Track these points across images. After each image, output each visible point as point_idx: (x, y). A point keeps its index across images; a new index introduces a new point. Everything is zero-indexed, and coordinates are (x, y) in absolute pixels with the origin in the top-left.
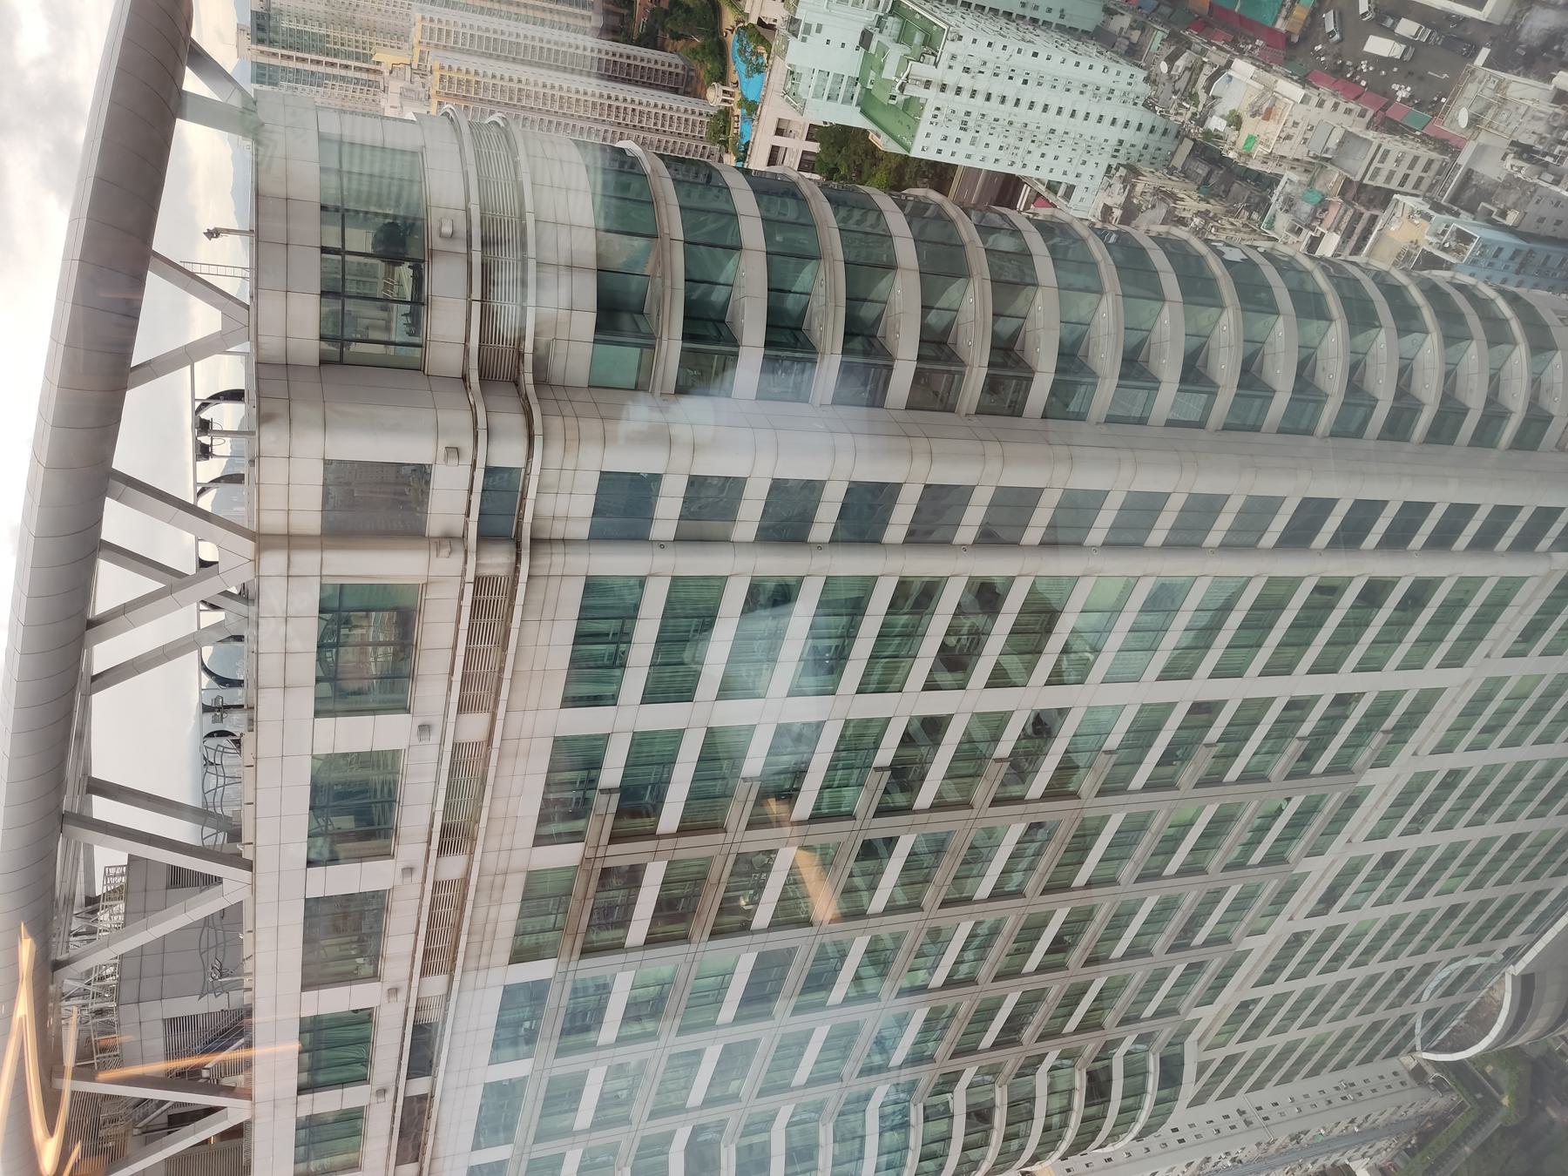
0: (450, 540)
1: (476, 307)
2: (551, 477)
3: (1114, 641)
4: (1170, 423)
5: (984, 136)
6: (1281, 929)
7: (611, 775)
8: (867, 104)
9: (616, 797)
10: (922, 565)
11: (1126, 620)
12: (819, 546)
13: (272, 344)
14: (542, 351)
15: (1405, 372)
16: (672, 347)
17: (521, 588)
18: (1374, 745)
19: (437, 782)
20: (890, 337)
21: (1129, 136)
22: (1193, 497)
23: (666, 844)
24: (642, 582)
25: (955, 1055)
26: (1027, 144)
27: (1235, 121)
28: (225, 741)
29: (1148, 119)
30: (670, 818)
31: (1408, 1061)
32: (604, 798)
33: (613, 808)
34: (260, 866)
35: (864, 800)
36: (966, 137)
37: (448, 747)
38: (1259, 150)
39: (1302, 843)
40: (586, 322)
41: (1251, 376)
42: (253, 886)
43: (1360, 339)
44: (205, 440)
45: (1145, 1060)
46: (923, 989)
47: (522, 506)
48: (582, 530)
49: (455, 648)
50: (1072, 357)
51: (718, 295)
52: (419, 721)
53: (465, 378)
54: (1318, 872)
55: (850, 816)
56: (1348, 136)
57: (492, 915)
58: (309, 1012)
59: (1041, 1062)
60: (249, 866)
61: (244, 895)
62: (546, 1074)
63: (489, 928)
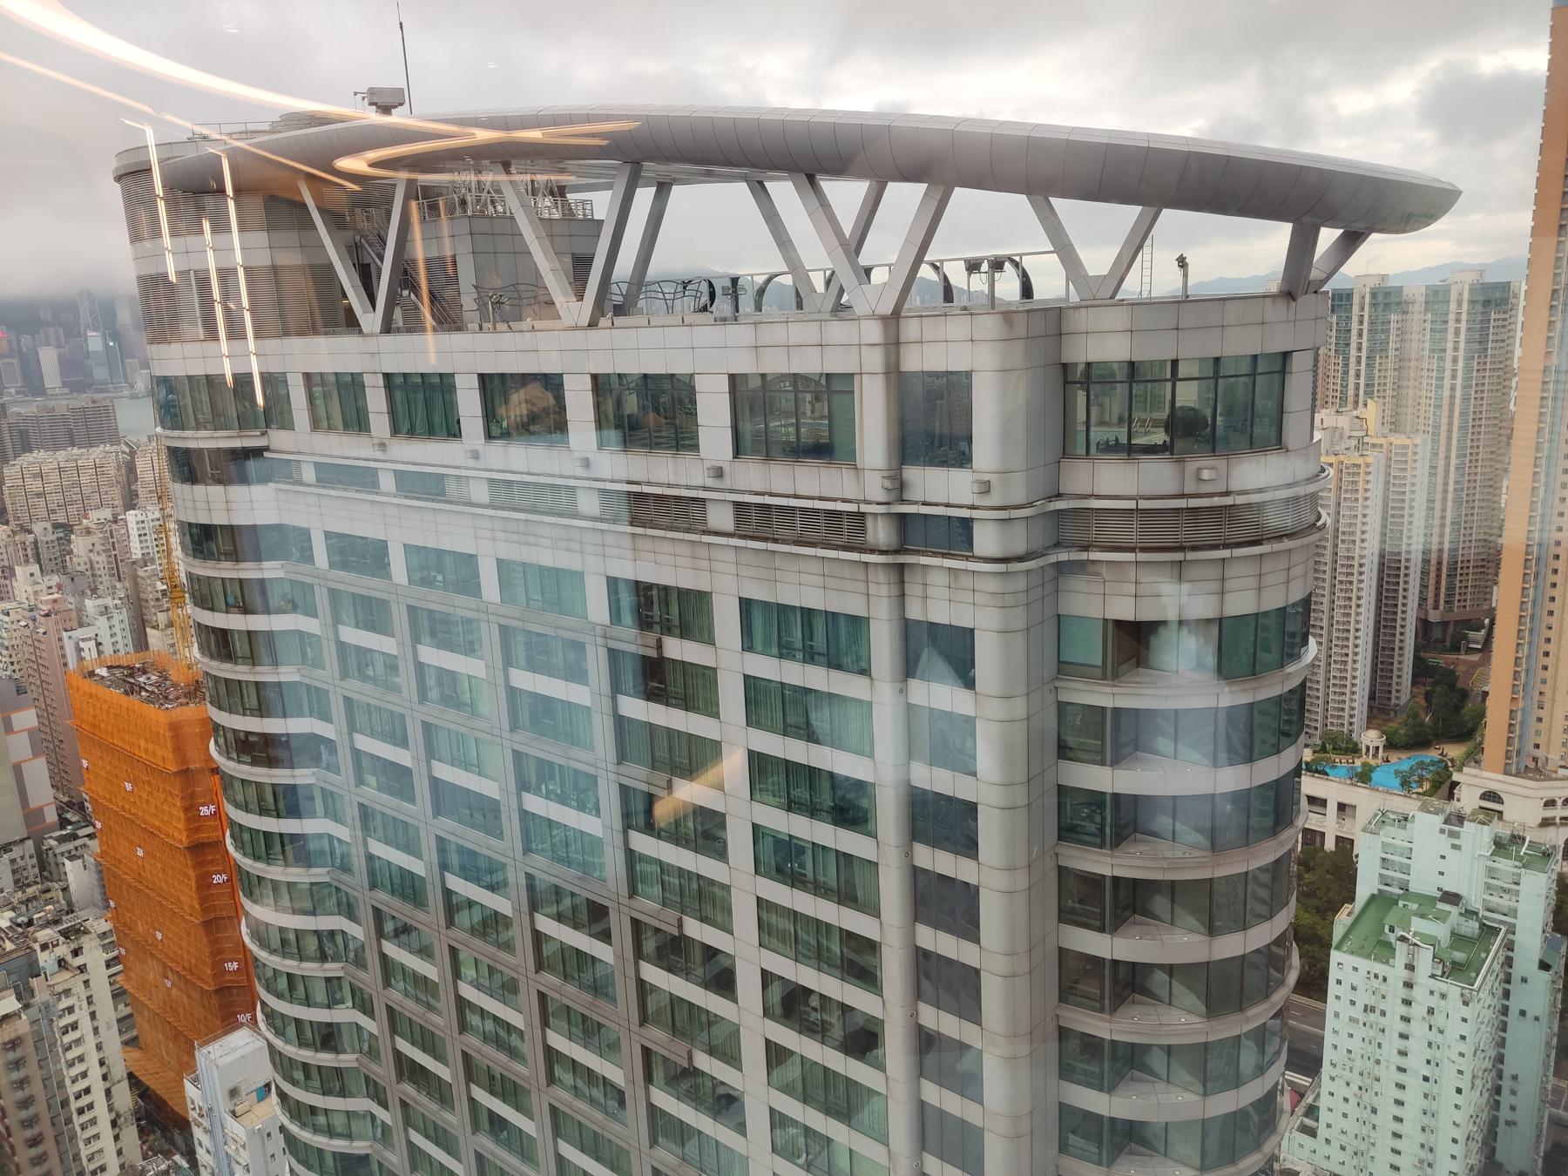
0: (899, 489)
1: (1131, 505)
2: (966, 581)
5: (1360, 1032)
8: (1382, 901)
10: (894, 968)
12: (909, 854)
13: (1081, 320)
14: (1091, 568)
19: (669, 486)
20: (1135, 930)
25: (390, 1010)
28: (705, 299)
32: (653, 642)
34: (592, 333)
35: (648, 907)
36: (1357, 1012)
40: (1124, 610)
42: (576, 328)
44: (985, 267)
46: (457, 975)
47: (935, 554)
48: (914, 612)
49: (796, 497)
51: (1164, 744)
52: (726, 467)
53: (1059, 496)
55: (633, 893)
60: (593, 324)
61: (567, 320)
62: (393, 597)
63: (531, 539)
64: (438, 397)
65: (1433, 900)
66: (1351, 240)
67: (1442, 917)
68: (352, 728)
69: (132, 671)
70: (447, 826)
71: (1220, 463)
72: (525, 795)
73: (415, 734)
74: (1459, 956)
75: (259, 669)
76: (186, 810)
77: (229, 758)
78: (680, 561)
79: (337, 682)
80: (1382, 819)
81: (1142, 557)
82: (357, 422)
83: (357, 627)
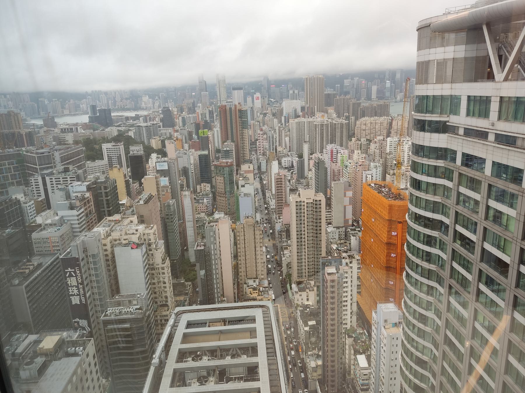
46: (475, 318)
59: (435, 347)
62: (483, 180)
68: (456, 222)
69: (381, 186)
70: (484, 267)
73: (480, 230)
75: (428, 195)
76: (388, 232)
77: (412, 221)
79: (454, 206)
82: (485, 114)
83: (467, 188)
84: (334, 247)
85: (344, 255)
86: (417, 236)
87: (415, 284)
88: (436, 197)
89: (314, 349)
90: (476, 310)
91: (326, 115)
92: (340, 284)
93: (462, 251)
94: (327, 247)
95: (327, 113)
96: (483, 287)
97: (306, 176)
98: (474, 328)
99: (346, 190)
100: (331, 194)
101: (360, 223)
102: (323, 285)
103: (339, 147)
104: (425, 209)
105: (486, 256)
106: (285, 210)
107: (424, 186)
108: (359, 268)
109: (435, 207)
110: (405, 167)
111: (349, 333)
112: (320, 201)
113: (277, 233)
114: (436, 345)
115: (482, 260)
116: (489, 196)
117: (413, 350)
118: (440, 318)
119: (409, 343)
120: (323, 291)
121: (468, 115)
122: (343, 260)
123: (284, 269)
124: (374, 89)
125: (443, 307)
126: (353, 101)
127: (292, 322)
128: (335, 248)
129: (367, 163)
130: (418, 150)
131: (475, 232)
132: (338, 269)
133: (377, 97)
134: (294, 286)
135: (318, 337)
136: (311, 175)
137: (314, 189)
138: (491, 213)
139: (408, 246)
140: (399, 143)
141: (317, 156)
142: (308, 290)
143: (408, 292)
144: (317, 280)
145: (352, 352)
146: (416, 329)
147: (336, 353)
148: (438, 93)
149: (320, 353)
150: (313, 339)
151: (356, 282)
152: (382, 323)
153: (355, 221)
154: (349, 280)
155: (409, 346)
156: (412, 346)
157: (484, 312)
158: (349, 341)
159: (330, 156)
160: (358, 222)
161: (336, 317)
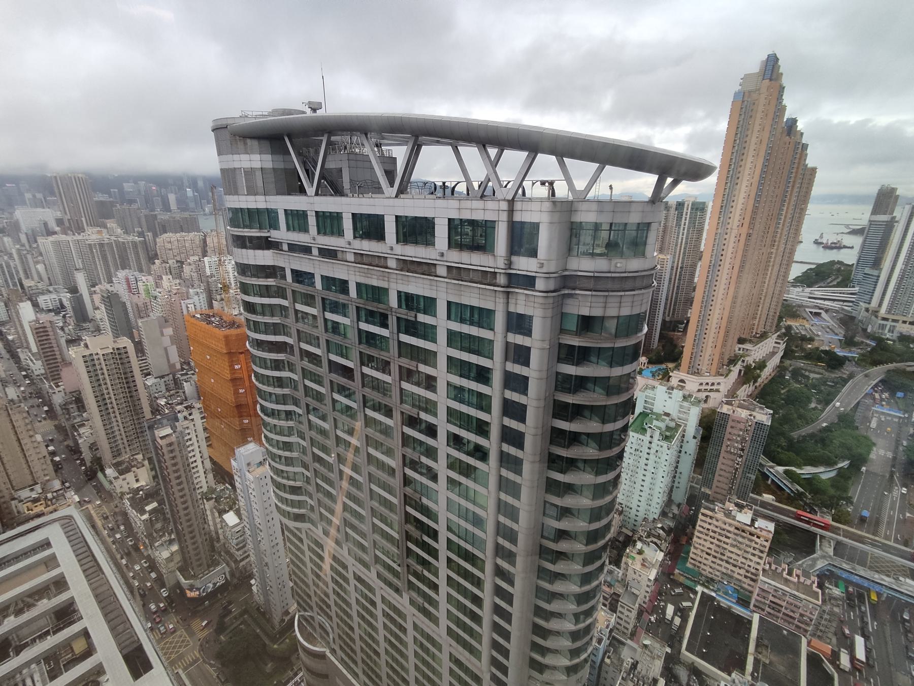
0: (509, 265)
1: (592, 274)
2: (532, 299)
3: (463, 502)
4: (543, 524)
5: (633, 457)
6: (350, 561)
7: (422, 318)
8: (644, 415)
9: (413, 319)
10: (495, 432)
11: (471, 506)
12: (503, 393)
15: (560, 616)
16: (576, 342)
17: (492, 288)
18: (418, 599)
19: (423, 258)
20: (578, 421)
21: (633, 512)
22: (517, 533)
23: (395, 337)
24: (492, 329)
26: (630, 473)
27: (640, 552)
28: (433, 189)
29: (640, 519)
30: (405, 338)
31: (293, 607)
32: (414, 315)
33: (409, 318)
34: (396, 200)
35: (407, 408)
36: (632, 451)
37: (435, 262)
38: (630, 561)
39: (382, 570)
40: (585, 312)
41: (560, 556)
42: (390, 198)
43: (573, 598)
44: (547, 184)
45: (304, 508)
46: (336, 427)
47: (521, 289)
48: (512, 309)
49: (471, 265)
50: (569, 489)
52: (445, 252)
54: (371, 576)
55: (402, 402)
56: (637, 596)
57: (374, 277)
58: (344, 215)
60: (396, 197)
61: (387, 195)
63: (369, 275)
64: (336, 222)
65: (661, 415)
66: (675, 183)
67: (663, 421)
68: (299, 340)
69: (209, 316)
71: (623, 261)
72: (363, 367)
74: (668, 434)
76: (230, 366)
78: (425, 286)
80: (647, 387)
81: (594, 293)
82: (304, 229)
84: (162, 402)
85: (179, 408)
86: (263, 363)
87: (273, 414)
88: (274, 318)
89: (164, 535)
90: (335, 419)
91: (105, 231)
92: (180, 445)
93: (311, 367)
94: (151, 406)
95: (105, 227)
96: (336, 396)
97: (90, 317)
98: (337, 436)
99: (161, 327)
100: (140, 336)
101: (192, 364)
102: (157, 454)
103: (137, 273)
104: (266, 333)
105: (334, 367)
106: (65, 373)
107: (259, 309)
108: (202, 418)
109: (276, 329)
110: (234, 291)
111: (206, 497)
112: (125, 348)
113: (58, 408)
114: (305, 466)
115: (330, 372)
116: (324, 310)
117: (284, 481)
118: (304, 439)
119: (278, 476)
120: (159, 462)
121: (288, 229)
122: (179, 415)
123: (87, 455)
124: (172, 198)
125: (304, 428)
126: (145, 212)
127: (120, 518)
128: (163, 403)
129: (184, 289)
130: (243, 269)
131: (319, 347)
132: (174, 428)
133: (178, 208)
134: (110, 472)
135: (165, 519)
136: (101, 315)
137: (111, 334)
138: (330, 325)
139: (255, 376)
140: (220, 263)
141: (103, 288)
142: (134, 469)
143: (266, 425)
144: (144, 451)
145: (217, 514)
146: (283, 459)
147: (195, 526)
148: (252, 206)
149: (173, 537)
150: (159, 526)
151: (202, 435)
152: (245, 468)
153: (184, 363)
154: (193, 436)
155: (279, 480)
156: (283, 478)
157: (343, 419)
158: (208, 505)
159: (125, 286)
160: (189, 364)
161: (185, 485)
